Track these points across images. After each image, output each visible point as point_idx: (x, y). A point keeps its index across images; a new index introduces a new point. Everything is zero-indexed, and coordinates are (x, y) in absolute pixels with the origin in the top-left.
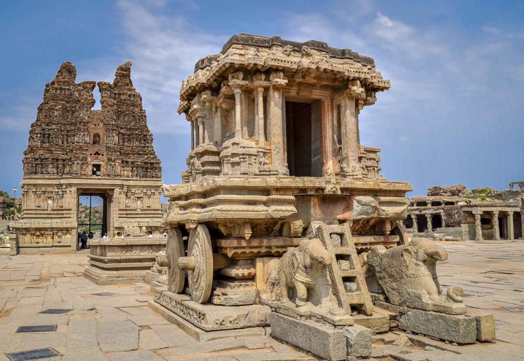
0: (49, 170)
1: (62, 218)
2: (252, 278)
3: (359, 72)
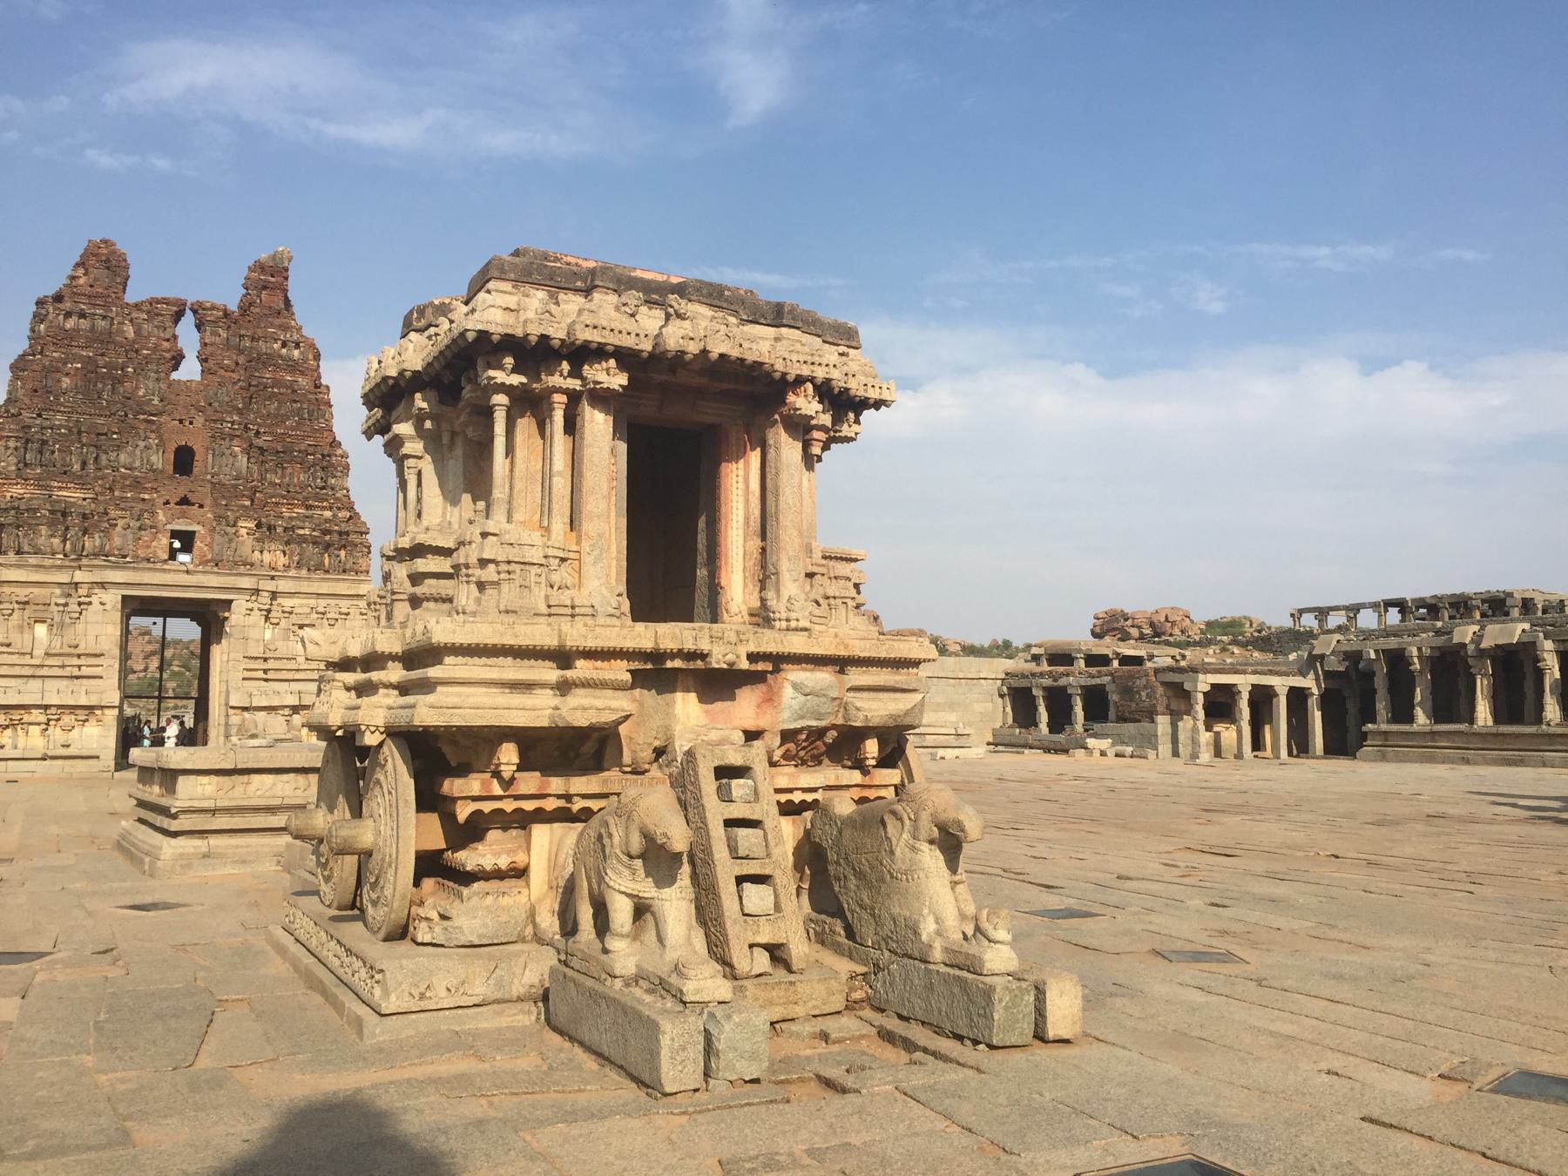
0: (41, 541)
1: (77, 677)
2: (520, 873)
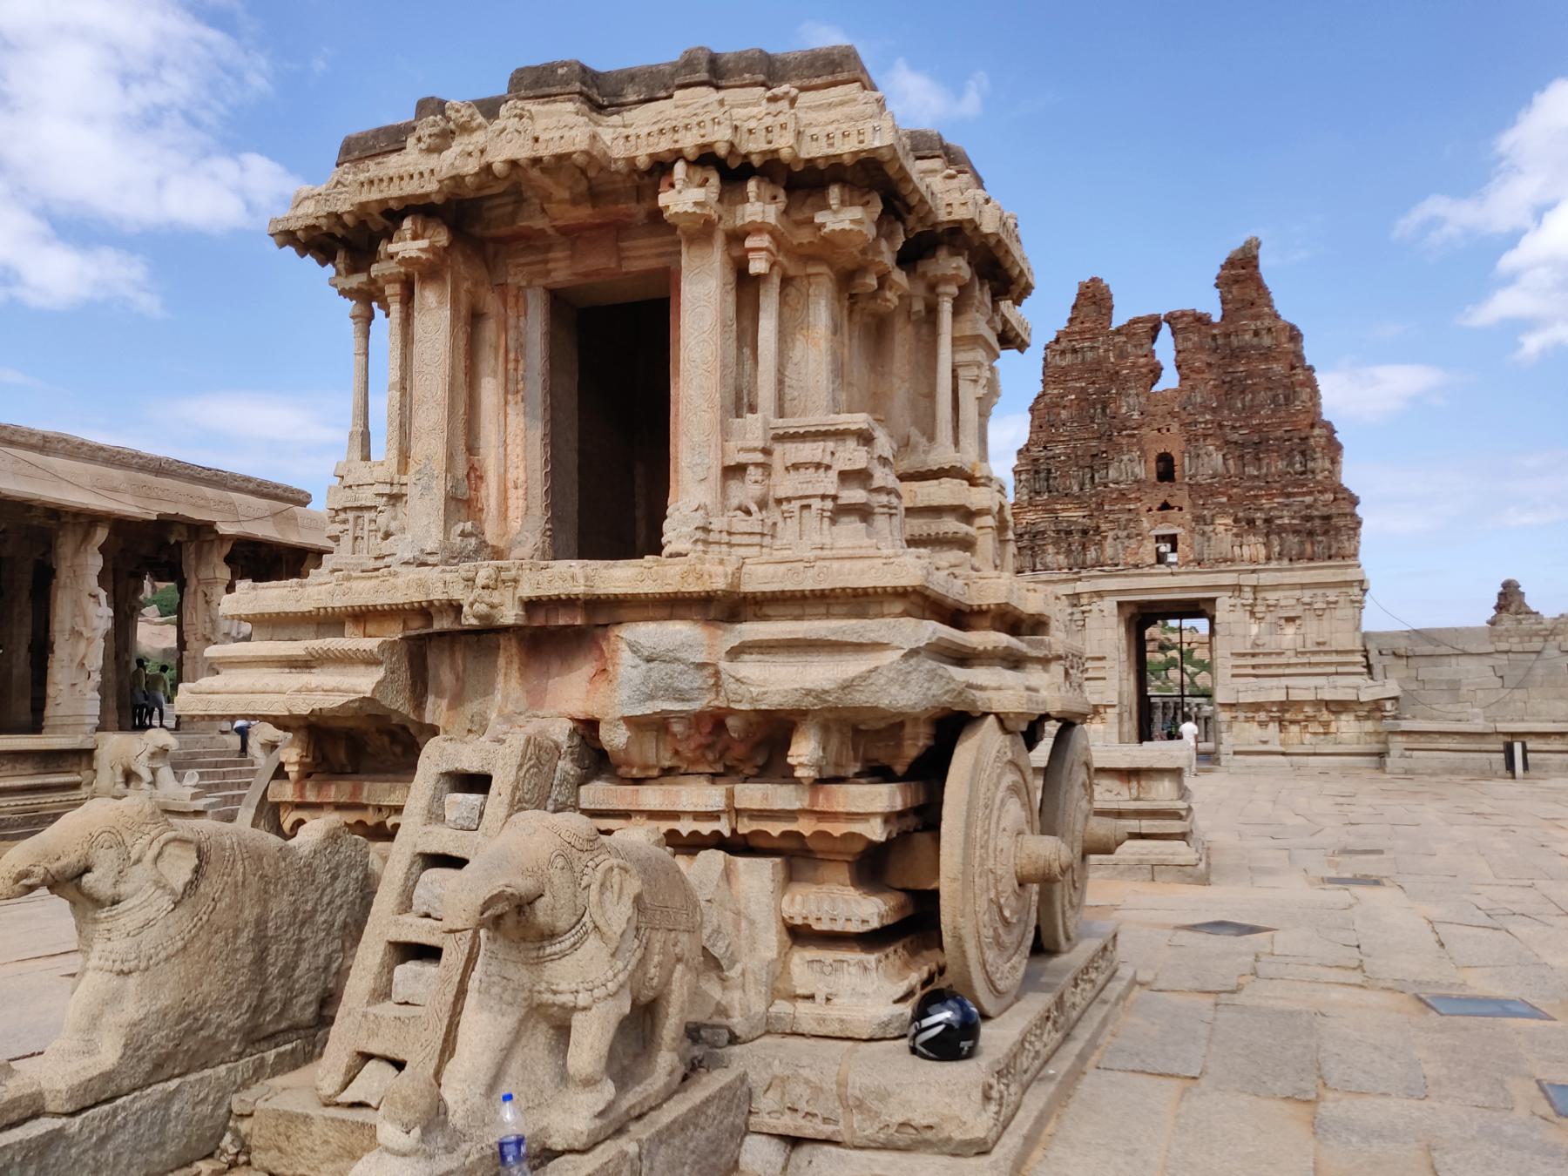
0: (1049, 559)
3: (675, 130)
